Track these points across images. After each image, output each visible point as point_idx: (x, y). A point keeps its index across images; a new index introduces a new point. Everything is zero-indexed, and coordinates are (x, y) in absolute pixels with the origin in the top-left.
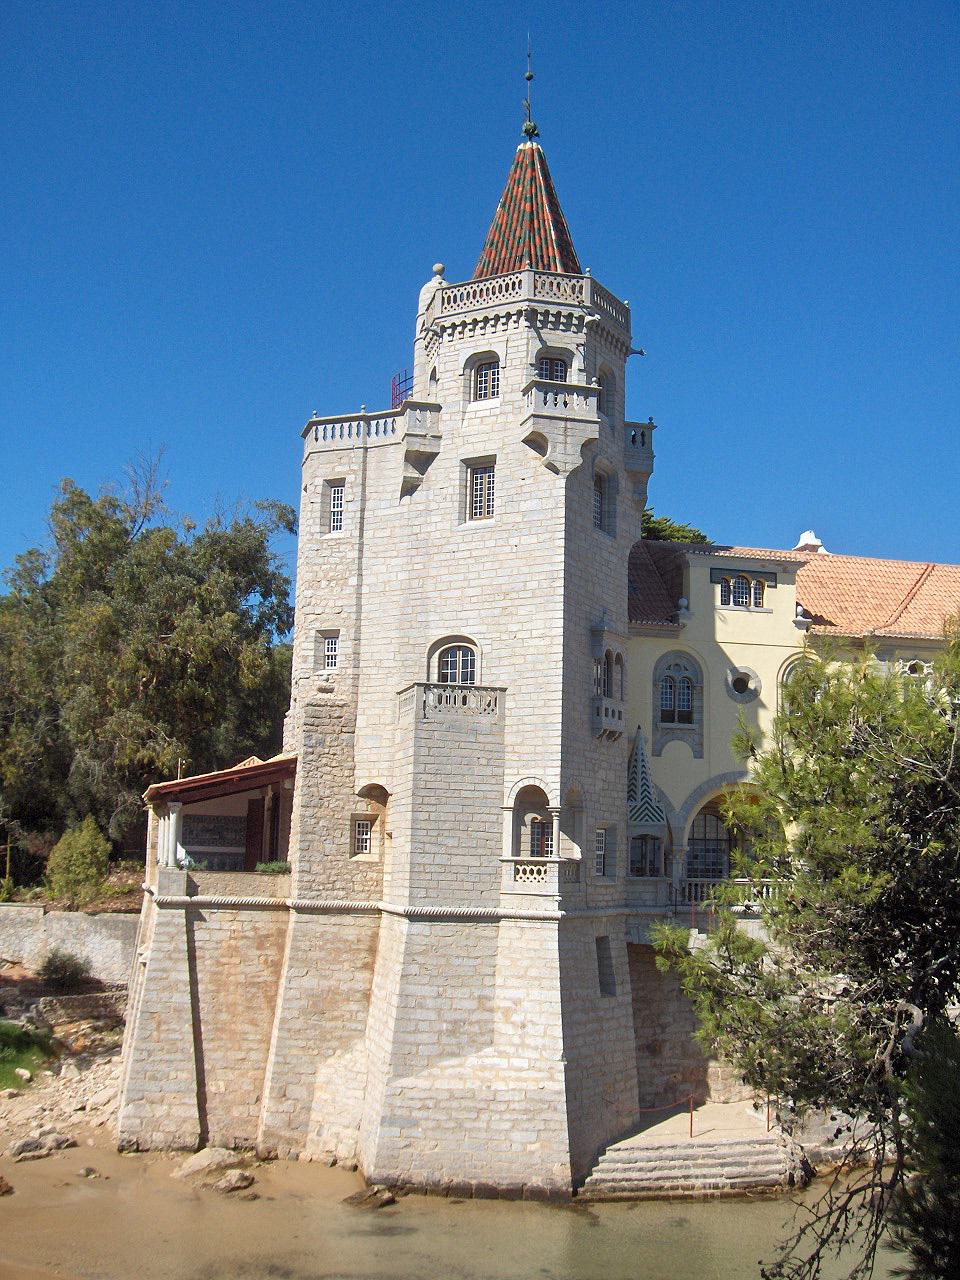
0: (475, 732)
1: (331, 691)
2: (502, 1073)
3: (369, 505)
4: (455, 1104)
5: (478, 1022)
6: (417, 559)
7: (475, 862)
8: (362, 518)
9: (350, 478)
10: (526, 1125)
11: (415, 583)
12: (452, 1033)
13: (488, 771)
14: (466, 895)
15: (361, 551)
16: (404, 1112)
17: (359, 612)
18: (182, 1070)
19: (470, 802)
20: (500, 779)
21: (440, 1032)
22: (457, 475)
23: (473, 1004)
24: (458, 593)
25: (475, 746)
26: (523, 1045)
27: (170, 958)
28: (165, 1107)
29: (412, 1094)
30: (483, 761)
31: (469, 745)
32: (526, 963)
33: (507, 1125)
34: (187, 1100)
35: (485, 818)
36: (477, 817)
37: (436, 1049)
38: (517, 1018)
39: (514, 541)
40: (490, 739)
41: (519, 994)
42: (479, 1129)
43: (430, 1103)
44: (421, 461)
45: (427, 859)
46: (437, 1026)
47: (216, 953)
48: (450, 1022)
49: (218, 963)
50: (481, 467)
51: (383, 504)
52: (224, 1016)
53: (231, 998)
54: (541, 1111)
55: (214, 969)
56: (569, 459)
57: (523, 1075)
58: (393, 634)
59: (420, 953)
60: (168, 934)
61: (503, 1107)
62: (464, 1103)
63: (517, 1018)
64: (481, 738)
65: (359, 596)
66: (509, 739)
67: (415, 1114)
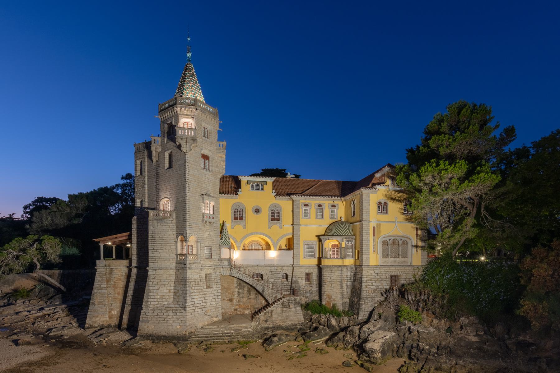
2: (172, 309)
4: (159, 316)
5: (168, 296)
7: (168, 255)
10: (176, 321)
12: (160, 298)
13: (171, 232)
14: (165, 264)
16: (146, 319)
18: (104, 309)
19: (166, 241)
21: (157, 299)
23: (167, 291)
25: (167, 226)
26: (179, 301)
27: (100, 282)
28: (99, 318)
29: (147, 314)
31: (165, 226)
32: (181, 280)
33: (171, 322)
34: (105, 316)
35: (171, 245)
36: (168, 245)
37: (157, 303)
38: (178, 295)
41: (179, 288)
42: (164, 323)
43: (152, 316)
45: (155, 255)
46: (156, 297)
47: (115, 280)
48: (160, 296)
49: (115, 282)
52: (117, 295)
53: (119, 291)
54: (180, 318)
55: (114, 284)
57: (178, 309)
59: (152, 279)
60: (100, 276)
61: (171, 317)
62: (161, 316)
63: (178, 295)
67: (149, 319)
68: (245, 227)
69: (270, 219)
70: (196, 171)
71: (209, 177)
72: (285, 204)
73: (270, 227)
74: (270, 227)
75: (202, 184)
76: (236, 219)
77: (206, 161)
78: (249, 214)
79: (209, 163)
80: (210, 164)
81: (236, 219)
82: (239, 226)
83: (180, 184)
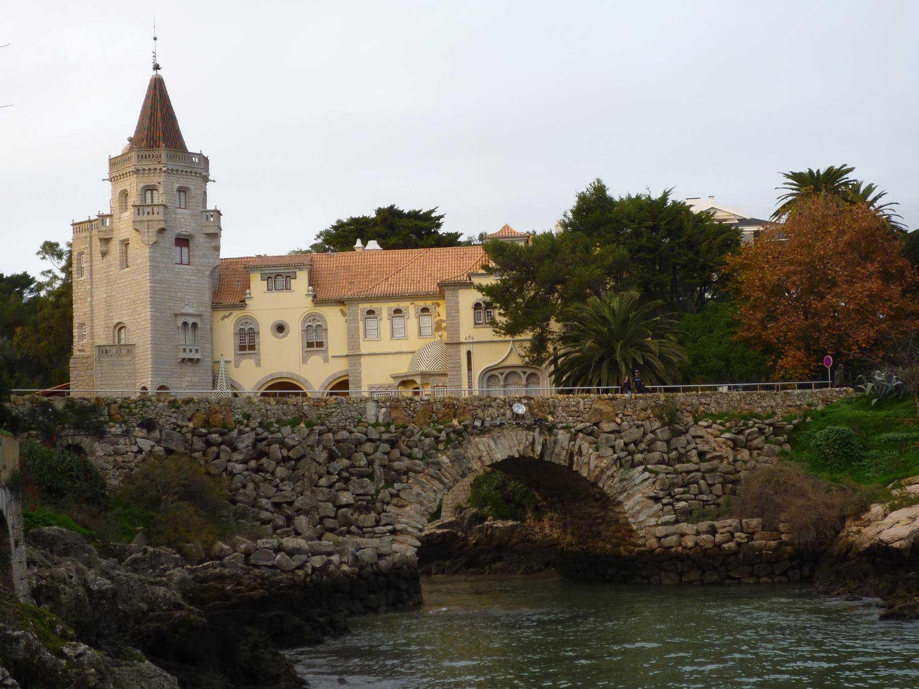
0: (123, 365)
1: (83, 351)
3: (94, 263)
6: (109, 288)
8: (91, 270)
9: (86, 251)
11: (109, 298)
15: (91, 285)
17: (92, 313)
20: (134, 385)
22: (118, 248)
24: (120, 302)
30: (126, 378)
39: (135, 278)
40: (129, 367)
44: (106, 241)
50: (125, 243)
51: (98, 263)
56: (150, 239)
58: (103, 323)
64: (125, 368)
65: (92, 306)
66: (138, 367)
68: (258, 364)
69: (306, 344)
70: (166, 271)
71: (188, 277)
72: (333, 317)
73: (305, 360)
74: (305, 360)
75: (176, 292)
76: (242, 348)
77: (185, 250)
78: (266, 338)
79: (189, 251)
80: (191, 254)
81: (242, 348)
82: (248, 363)
83: (141, 297)
